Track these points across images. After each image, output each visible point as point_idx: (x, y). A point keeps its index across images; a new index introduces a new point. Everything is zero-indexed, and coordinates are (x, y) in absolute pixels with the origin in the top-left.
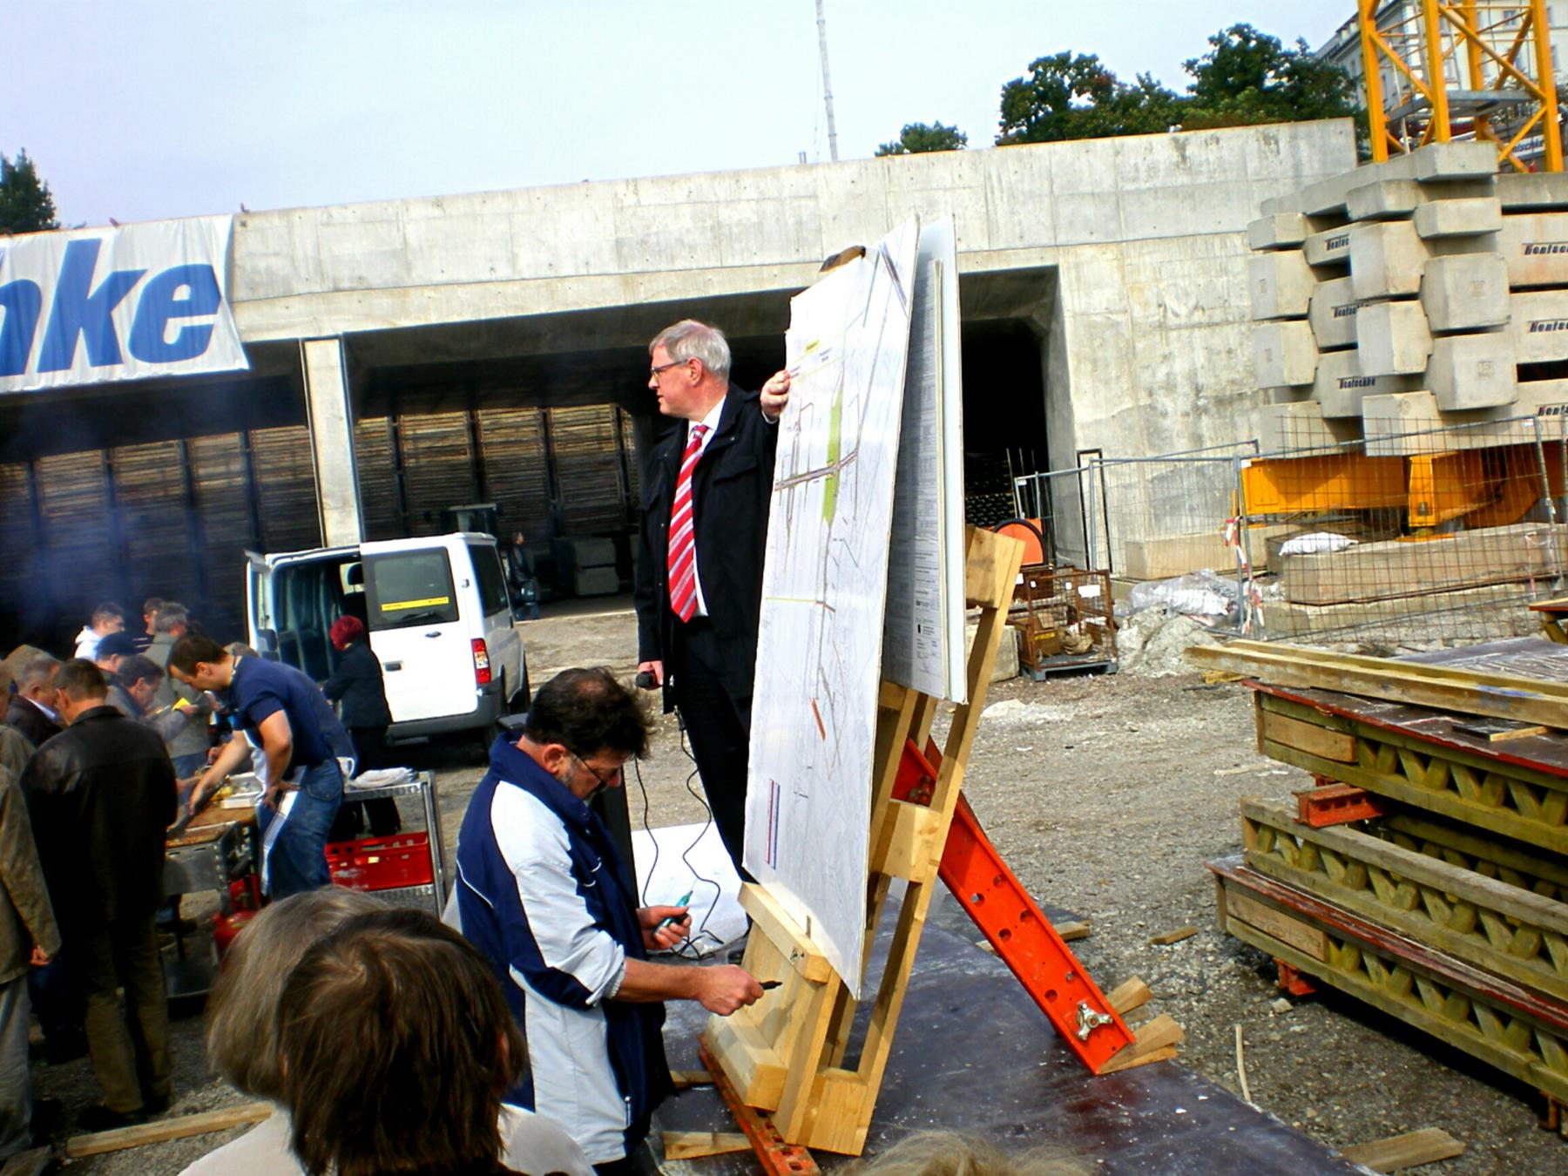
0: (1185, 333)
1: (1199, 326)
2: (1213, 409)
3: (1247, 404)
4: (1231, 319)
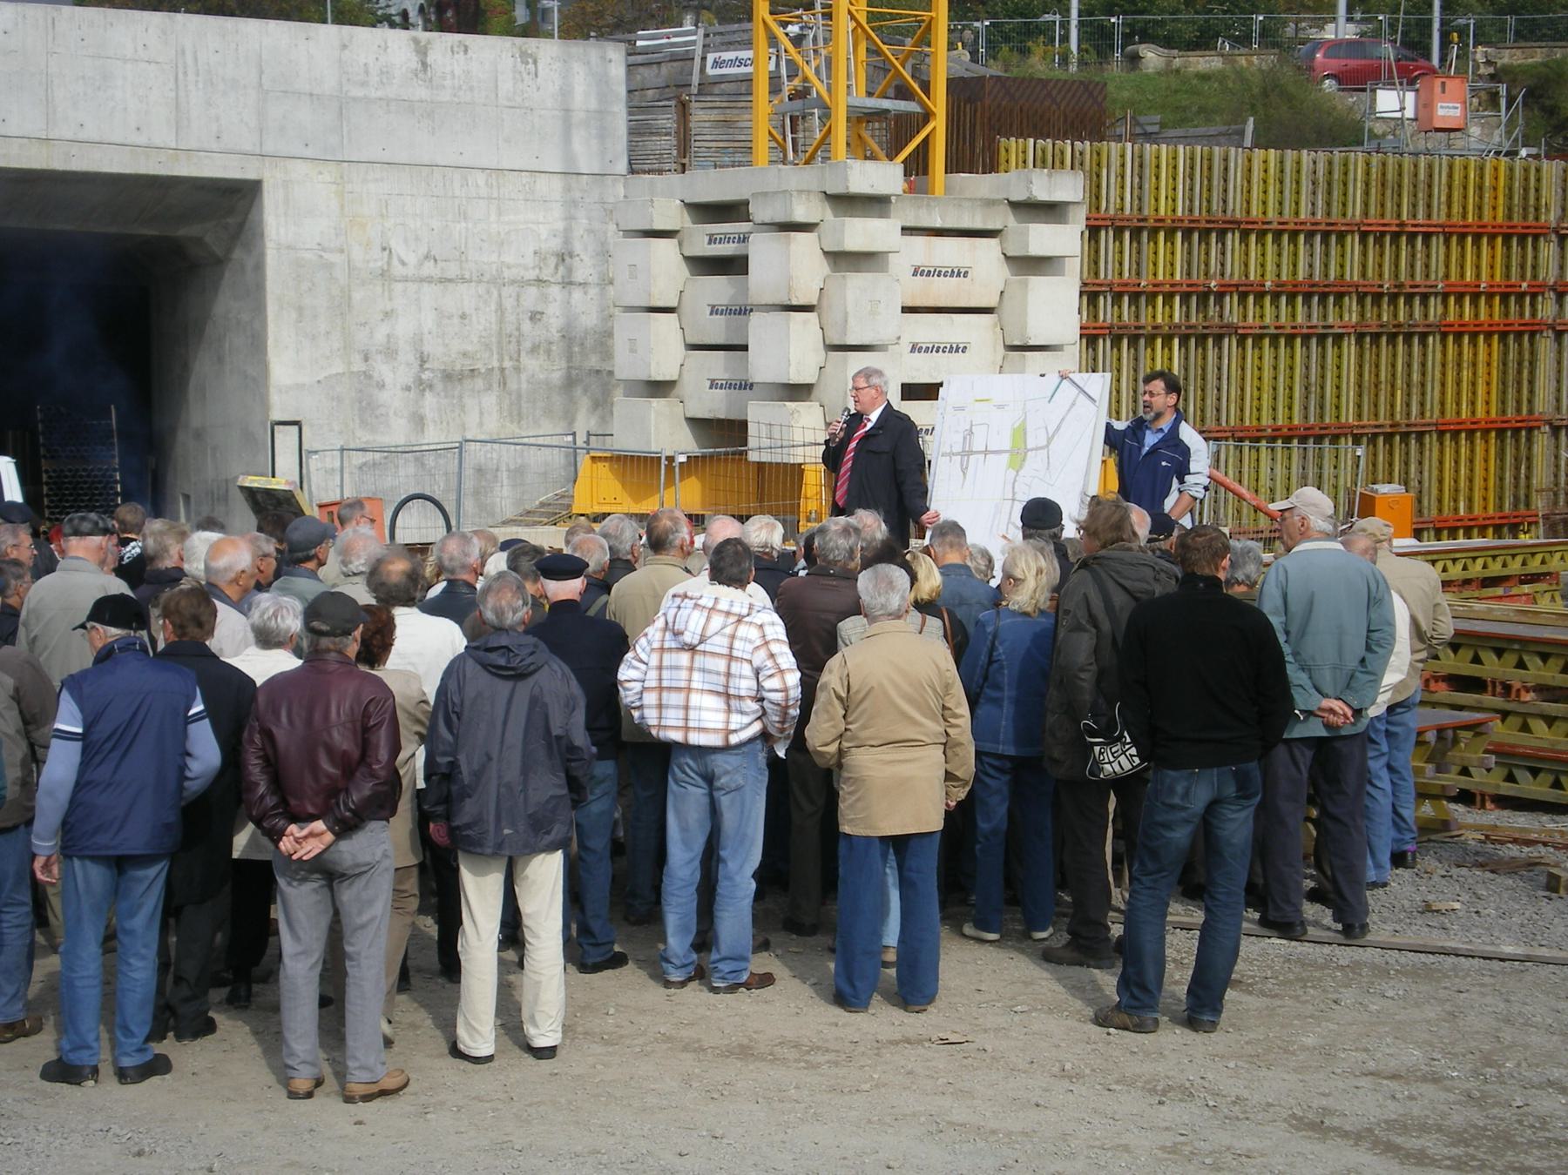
0: (412, 287)
1: (429, 280)
2: (439, 386)
3: (479, 383)
4: (467, 276)
